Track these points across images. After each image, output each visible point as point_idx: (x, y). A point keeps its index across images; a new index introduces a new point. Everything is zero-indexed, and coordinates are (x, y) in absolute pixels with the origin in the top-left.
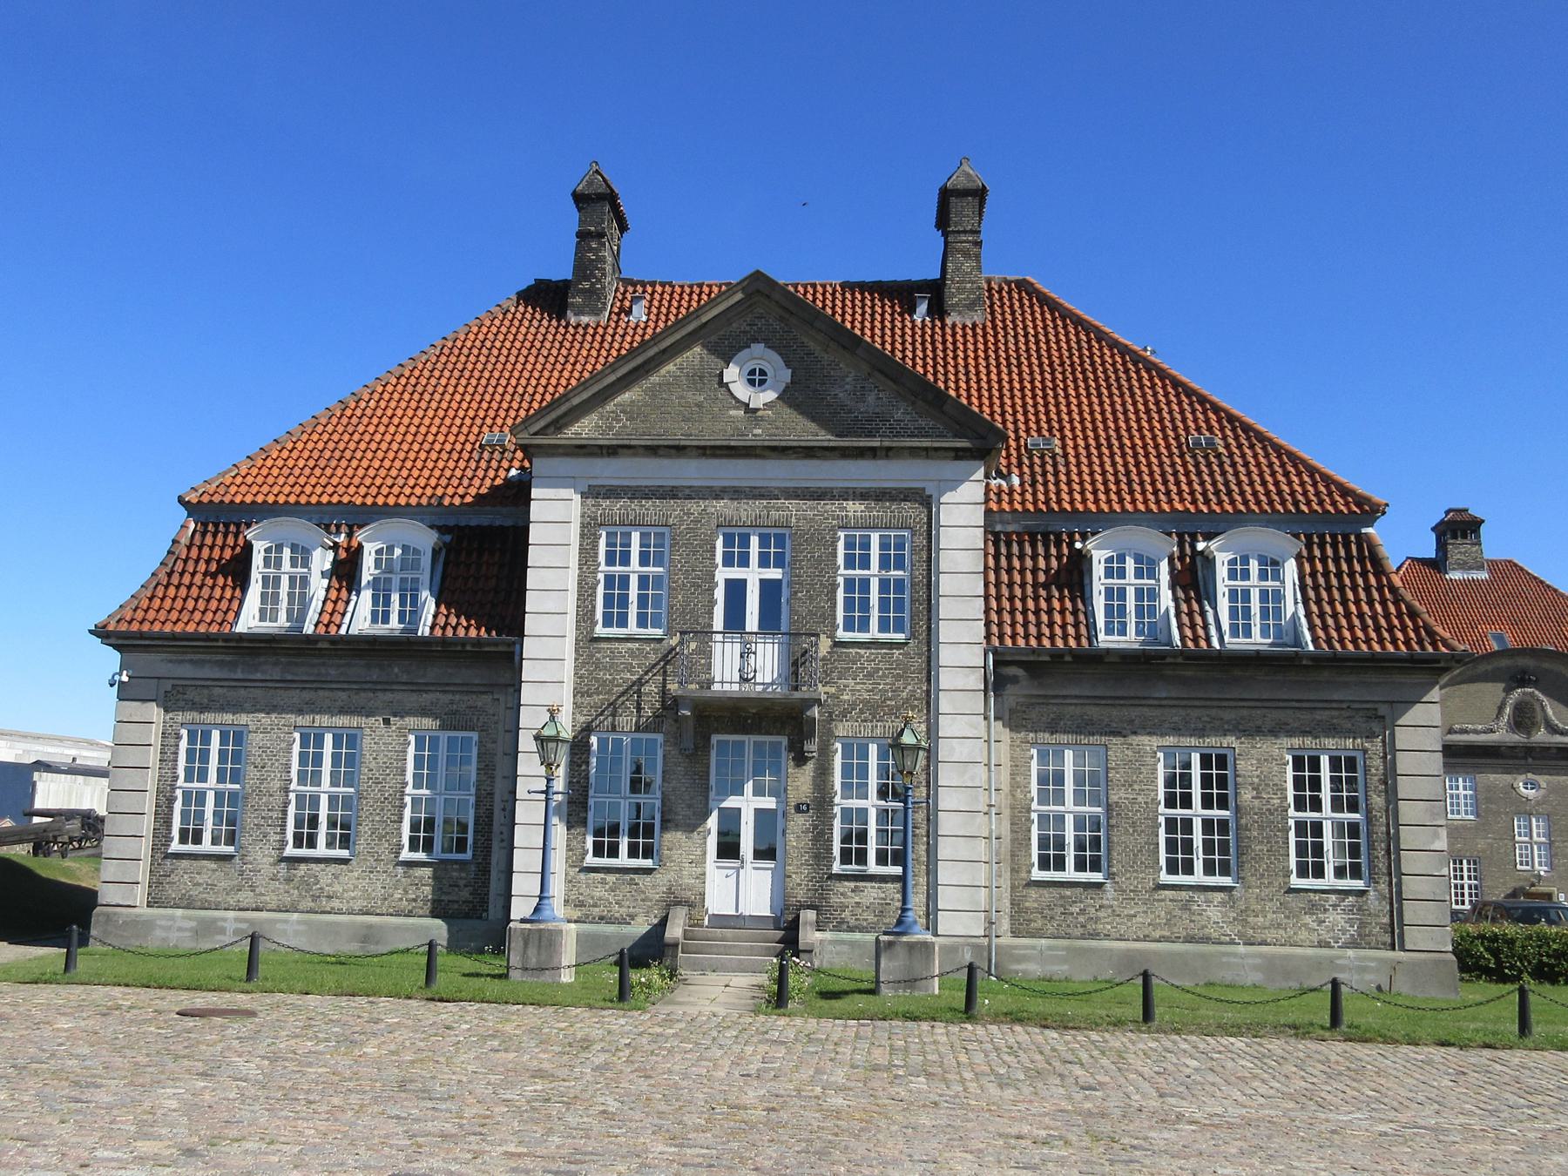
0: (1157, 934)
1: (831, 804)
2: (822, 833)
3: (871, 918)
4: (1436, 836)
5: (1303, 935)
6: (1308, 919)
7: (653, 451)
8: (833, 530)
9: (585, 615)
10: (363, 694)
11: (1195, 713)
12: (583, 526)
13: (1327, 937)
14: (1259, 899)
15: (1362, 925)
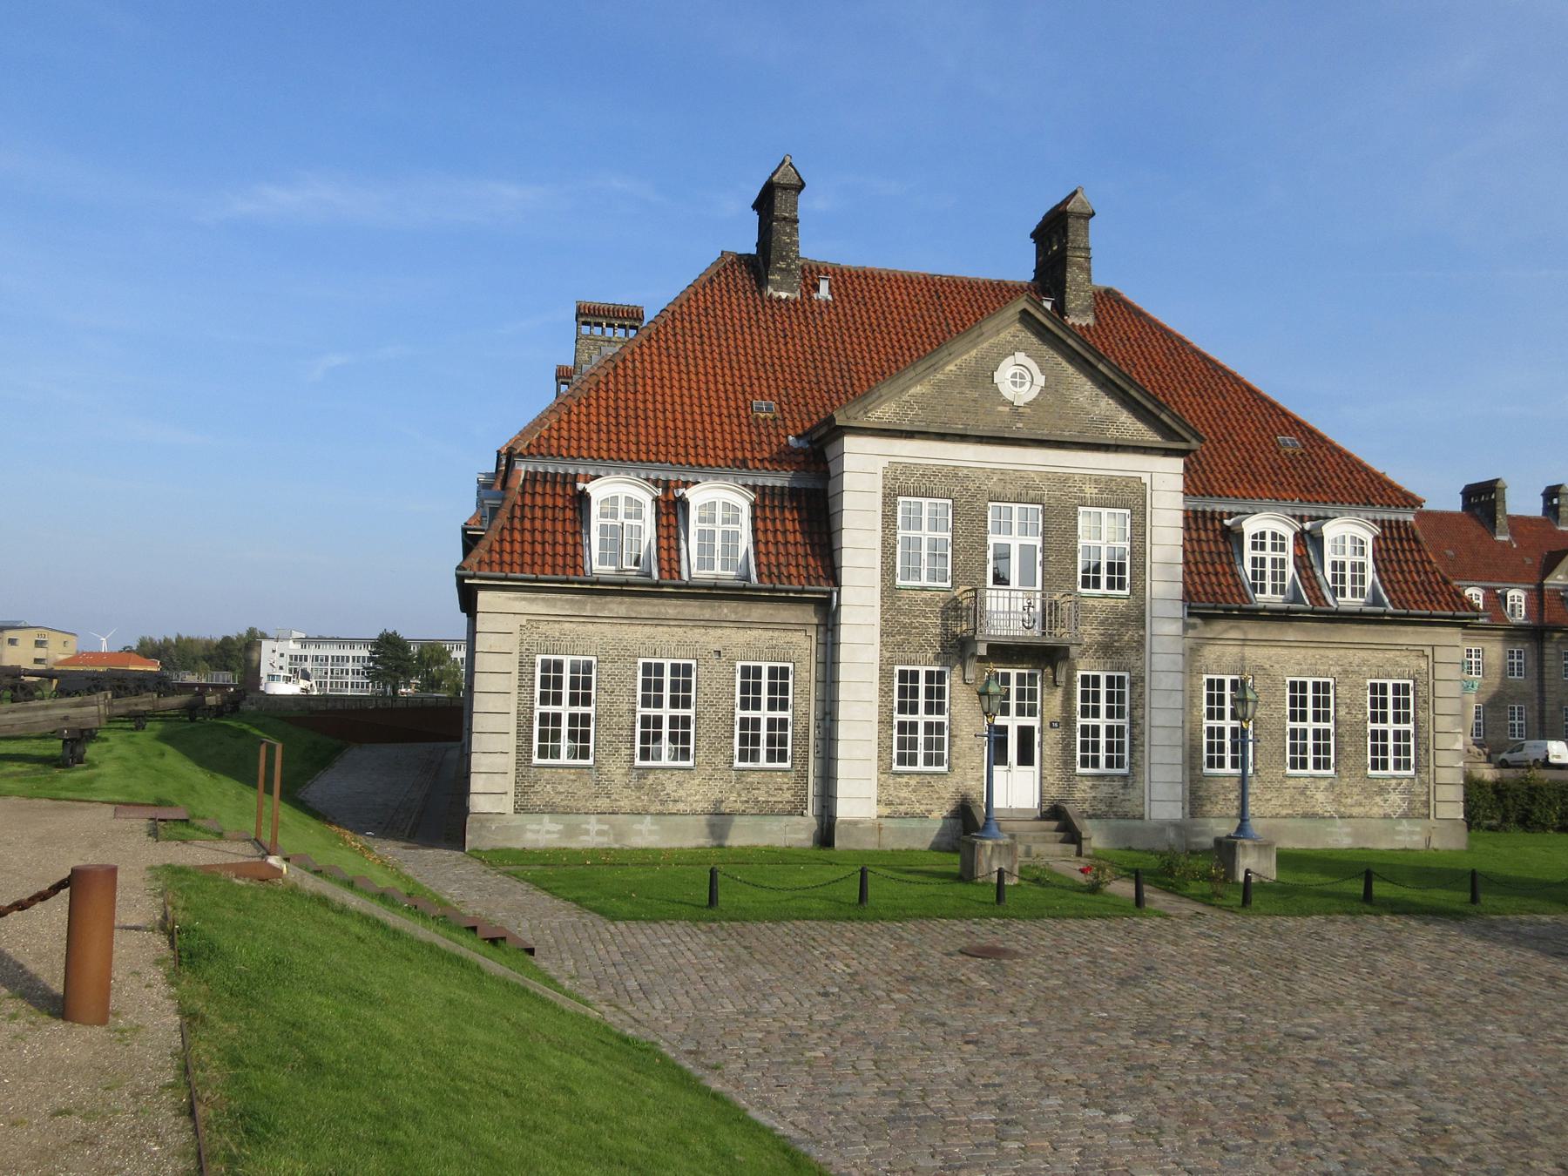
0: (1284, 812)
1: (1075, 722)
2: (1068, 745)
3: (1104, 808)
4: (1456, 740)
5: (1375, 810)
6: (1378, 799)
7: (942, 437)
8: (1075, 508)
9: (888, 570)
10: (697, 631)
11: (1311, 652)
12: (884, 496)
13: (1389, 811)
14: (1348, 785)
15: (1411, 802)
